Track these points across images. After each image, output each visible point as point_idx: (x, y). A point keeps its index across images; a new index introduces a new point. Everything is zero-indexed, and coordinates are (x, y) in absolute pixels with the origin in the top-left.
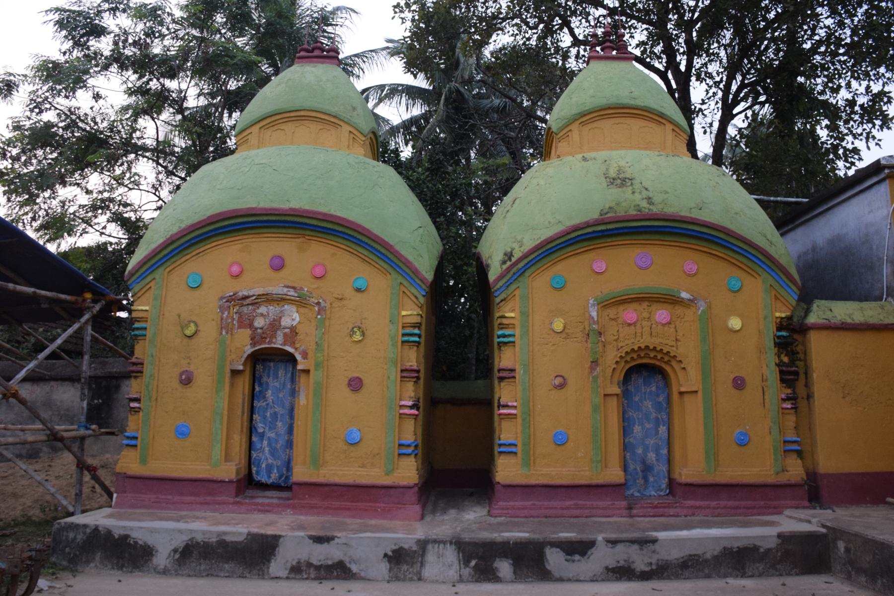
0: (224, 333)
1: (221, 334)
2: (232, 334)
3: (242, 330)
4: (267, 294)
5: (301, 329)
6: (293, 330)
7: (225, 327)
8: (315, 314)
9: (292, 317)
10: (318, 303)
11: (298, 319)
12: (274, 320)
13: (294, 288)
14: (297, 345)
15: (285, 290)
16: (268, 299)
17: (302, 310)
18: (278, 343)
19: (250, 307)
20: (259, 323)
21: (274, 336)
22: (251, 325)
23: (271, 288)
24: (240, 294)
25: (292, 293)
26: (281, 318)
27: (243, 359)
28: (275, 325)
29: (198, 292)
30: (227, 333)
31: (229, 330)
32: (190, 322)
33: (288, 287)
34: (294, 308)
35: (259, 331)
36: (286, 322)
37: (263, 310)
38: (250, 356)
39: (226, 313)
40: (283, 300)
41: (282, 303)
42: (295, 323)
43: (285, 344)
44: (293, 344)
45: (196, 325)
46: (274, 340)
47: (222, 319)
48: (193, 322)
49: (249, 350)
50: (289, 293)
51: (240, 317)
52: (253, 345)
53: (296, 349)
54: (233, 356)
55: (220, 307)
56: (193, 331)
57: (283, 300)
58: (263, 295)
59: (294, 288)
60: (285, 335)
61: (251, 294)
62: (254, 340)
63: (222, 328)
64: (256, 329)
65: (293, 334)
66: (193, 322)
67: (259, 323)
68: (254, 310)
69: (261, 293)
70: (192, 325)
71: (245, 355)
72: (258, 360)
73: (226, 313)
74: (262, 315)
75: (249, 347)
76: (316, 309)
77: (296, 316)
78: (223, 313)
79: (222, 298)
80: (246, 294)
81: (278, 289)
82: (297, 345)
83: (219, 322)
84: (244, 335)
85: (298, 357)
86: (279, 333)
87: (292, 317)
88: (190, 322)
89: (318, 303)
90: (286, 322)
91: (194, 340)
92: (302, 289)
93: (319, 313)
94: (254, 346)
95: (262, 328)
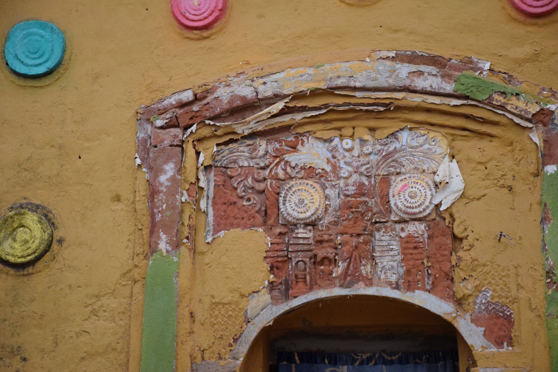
0: (163, 246)
1: (153, 249)
2: (194, 251)
3: (235, 232)
4: (330, 91)
5: (474, 223)
6: (443, 229)
7: (163, 222)
8: (533, 158)
9: (432, 174)
10: (543, 117)
11: (457, 184)
12: (361, 191)
13: (433, 61)
14: (462, 288)
15: (404, 70)
16: (336, 108)
17: (472, 147)
18: (384, 278)
19: (262, 146)
20: (302, 201)
21: (363, 252)
22: (268, 213)
23: (344, 67)
24: (224, 95)
25: (431, 80)
26: (386, 181)
27: (243, 349)
28: (365, 211)
29: (48, 96)
30: (176, 245)
31: (185, 239)
32: (21, 208)
33: (413, 59)
34: (438, 143)
35: (301, 232)
36: (410, 194)
37: (312, 152)
38: (265, 332)
39: (170, 168)
40: (390, 109)
41: (388, 126)
42: (446, 199)
43: (410, 287)
44: (443, 283)
45: (47, 218)
46: (366, 269)
47: (153, 192)
48: (35, 208)
49: (265, 311)
50: (420, 83)
51: (226, 180)
52: (281, 288)
53: (459, 302)
54: (204, 338)
55: (146, 148)
56: (35, 245)
57: (390, 109)
58: (315, 93)
59: (433, 61)
60: (410, 246)
61: (266, 91)
62: (282, 271)
63: (153, 227)
64: (291, 226)
65: (440, 241)
66: (35, 208)
67: (302, 201)
68: (278, 155)
69: (305, 87)
70: (31, 219)
71: (252, 333)
72: (291, 360)
73: (170, 168)
74: (310, 172)
75: (265, 297)
76: (536, 138)
77: (451, 172)
78: (155, 171)
79: (146, 115)
80: (247, 92)
81: (371, 71)
82: (462, 288)
83: (142, 206)
84: (251, 245)
85: (472, 334)
86: (382, 238)
87: (432, 174)
88: (21, 208)
89: (543, 117)
90: (410, 194)
91: (40, 279)
92: (468, 64)
93: (547, 157)
94: (287, 296)
95: (312, 224)
